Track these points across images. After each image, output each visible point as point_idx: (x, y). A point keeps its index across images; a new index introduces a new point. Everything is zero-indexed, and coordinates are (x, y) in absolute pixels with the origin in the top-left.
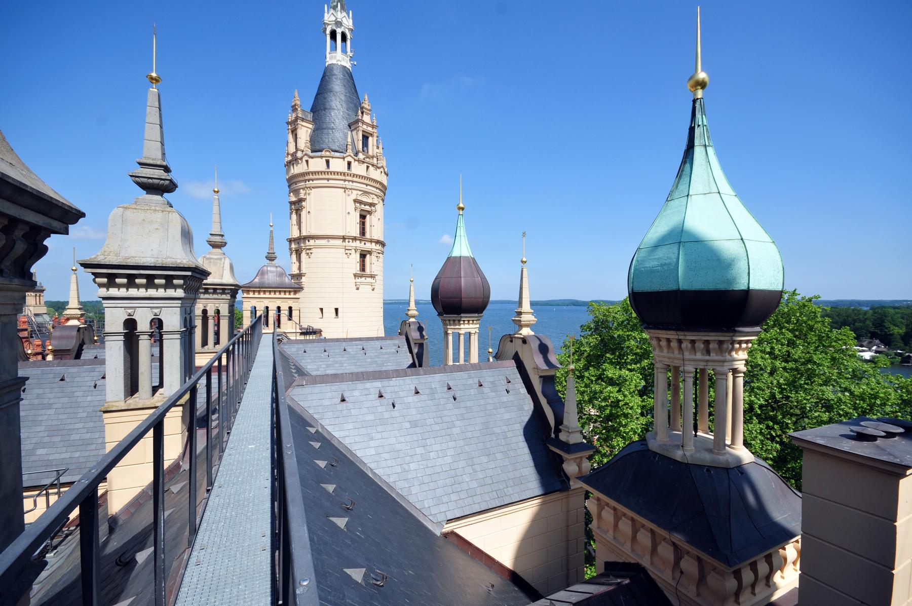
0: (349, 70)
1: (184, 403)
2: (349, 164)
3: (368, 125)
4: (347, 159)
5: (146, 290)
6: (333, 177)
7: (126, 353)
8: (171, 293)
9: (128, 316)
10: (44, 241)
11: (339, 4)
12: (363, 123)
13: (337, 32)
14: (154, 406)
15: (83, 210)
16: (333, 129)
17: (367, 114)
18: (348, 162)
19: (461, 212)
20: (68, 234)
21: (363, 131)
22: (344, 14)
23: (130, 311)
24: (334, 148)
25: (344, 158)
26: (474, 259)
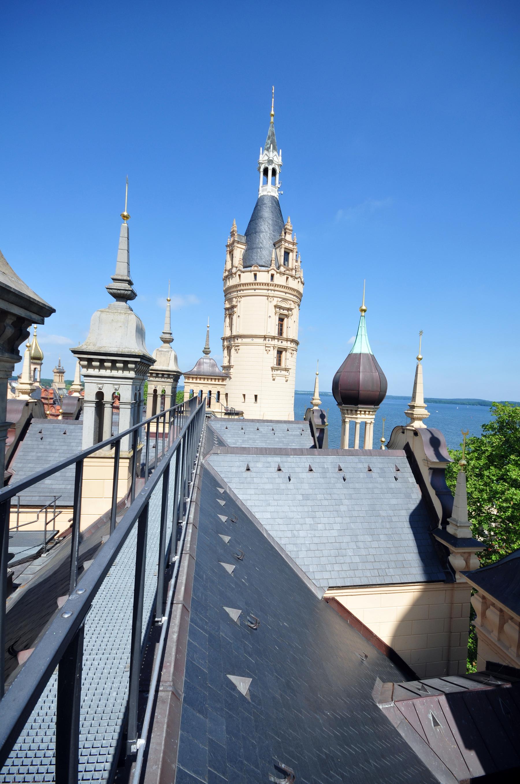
0: (277, 199)
1: (130, 457)
2: (272, 276)
3: (289, 242)
4: (270, 272)
5: (111, 371)
6: (259, 287)
7: (96, 416)
8: (127, 374)
9: (99, 389)
10: (27, 328)
11: (272, 145)
12: (286, 241)
13: (269, 169)
14: (111, 457)
15: (54, 307)
16: (261, 248)
17: (289, 234)
18: (271, 274)
19: (363, 314)
20: (43, 324)
21: (285, 248)
22: (275, 153)
23: (100, 386)
24: (261, 264)
25: (268, 271)
26: (373, 356)
